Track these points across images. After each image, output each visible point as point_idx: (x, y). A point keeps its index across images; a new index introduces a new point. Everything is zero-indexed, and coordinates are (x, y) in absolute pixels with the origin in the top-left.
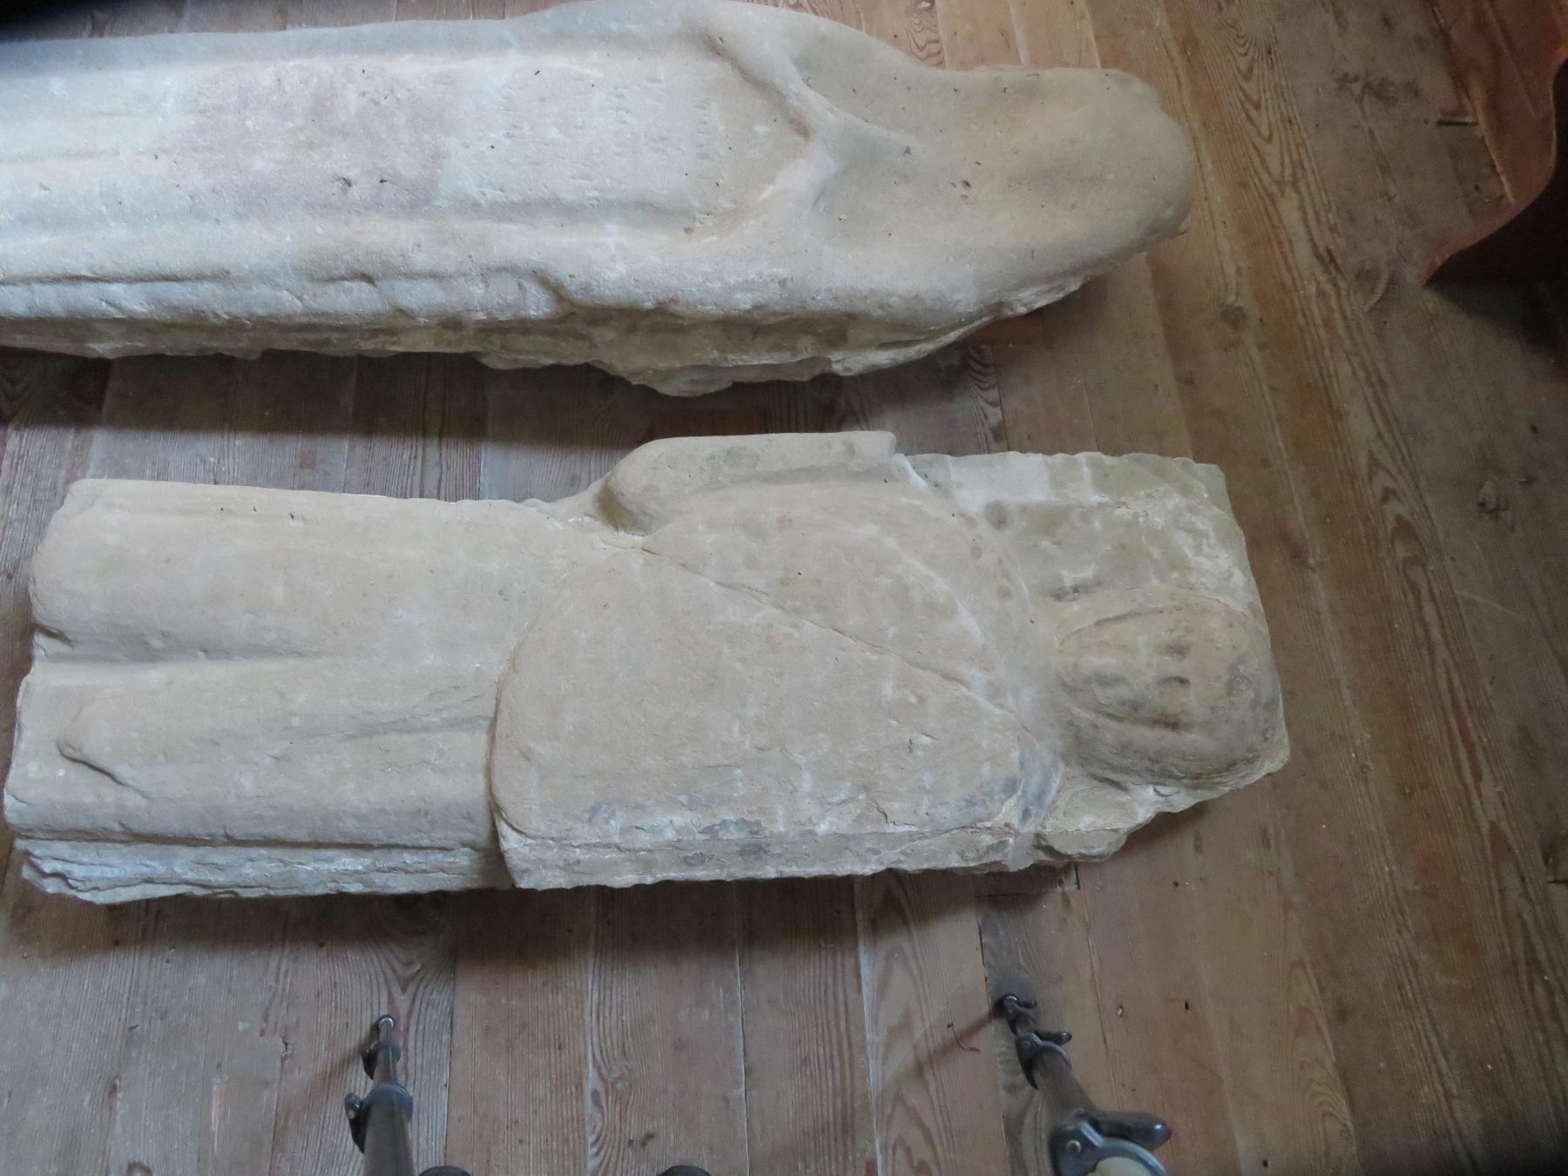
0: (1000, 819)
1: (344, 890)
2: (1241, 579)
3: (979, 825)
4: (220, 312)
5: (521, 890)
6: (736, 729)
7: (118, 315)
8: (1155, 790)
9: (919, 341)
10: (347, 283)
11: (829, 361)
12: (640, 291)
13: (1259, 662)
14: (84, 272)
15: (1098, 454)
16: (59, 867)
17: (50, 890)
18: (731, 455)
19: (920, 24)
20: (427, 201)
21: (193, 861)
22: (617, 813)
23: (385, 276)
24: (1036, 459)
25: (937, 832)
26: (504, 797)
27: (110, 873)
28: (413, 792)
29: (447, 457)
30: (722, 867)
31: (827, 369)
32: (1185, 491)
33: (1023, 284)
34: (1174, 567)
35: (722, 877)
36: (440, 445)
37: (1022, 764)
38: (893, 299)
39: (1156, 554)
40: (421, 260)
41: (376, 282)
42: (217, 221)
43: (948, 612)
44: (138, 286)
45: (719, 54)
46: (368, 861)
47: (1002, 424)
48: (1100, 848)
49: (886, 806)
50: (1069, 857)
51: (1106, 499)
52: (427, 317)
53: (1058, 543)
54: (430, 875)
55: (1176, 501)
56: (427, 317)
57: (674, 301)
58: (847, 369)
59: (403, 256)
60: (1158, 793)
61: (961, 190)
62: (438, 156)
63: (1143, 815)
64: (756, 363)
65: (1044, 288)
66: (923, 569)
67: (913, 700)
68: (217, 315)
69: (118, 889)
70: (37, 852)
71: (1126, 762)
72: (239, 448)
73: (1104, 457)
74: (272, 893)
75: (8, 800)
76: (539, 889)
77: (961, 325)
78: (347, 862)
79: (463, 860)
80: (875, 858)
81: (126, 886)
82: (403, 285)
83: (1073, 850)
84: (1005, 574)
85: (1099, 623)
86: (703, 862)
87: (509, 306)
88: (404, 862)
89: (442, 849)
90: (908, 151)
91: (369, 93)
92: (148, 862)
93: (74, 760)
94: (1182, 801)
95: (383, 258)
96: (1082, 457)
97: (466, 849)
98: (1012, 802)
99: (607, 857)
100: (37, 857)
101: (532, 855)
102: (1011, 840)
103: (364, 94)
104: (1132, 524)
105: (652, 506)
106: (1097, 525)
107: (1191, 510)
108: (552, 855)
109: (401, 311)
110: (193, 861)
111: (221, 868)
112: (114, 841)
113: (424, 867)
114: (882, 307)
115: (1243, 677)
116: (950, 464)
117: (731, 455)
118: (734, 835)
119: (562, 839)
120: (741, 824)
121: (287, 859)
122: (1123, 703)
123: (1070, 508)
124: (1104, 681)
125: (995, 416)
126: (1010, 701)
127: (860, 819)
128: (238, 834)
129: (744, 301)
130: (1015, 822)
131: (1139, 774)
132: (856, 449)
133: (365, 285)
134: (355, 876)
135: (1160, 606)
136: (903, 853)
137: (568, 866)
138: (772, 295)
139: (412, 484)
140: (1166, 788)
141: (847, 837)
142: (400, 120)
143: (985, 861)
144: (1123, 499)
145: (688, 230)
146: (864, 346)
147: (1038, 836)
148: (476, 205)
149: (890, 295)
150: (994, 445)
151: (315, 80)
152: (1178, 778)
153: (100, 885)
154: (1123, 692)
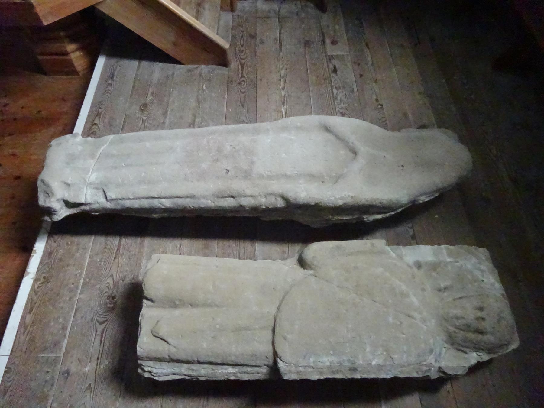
0: (428, 361)
1: (230, 379)
2: (498, 285)
3: (422, 363)
4: (191, 206)
5: (284, 379)
6: (346, 331)
7: (163, 207)
8: (476, 354)
9: (390, 212)
10: (227, 198)
11: (363, 218)
12: (311, 200)
13: (507, 313)
14: (156, 196)
15: (447, 246)
16: (149, 369)
17: (146, 376)
18: (338, 248)
21: (187, 369)
22: (312, 357)
23: (238, 196)
24: (429, 247)
25: (409, 365)
26: (279, 351)
27: (164, 371)
28: (251, 349)
29: (246, 246)
30: (344, 374)
31: (363, 220)
32: (477, 258)
33: (421, 195)
34: (475, 281)
35: (344, 377)
36: (244, 242)
37: (434, 344)
38: (384, 201)
39: (469, 277)
40: (248, 192)
41: (236, 198)
42: (192, 181)
43: (407, 296)
44: (170, 199)
46: (237, 370)
47: (414, 234)
48: (460, 372)
49: (393, 356)
50: (450, 375)
51: (451, 260)
52: (248, 207)
54: (255, 374)
55: (474, 260)
56: (248, 207)
57: (320, 203)
58: (368, 220)
59: (243, 191)
60: (478, 355)
61: (402, 168)
62: (252, 163)
63: (473, 362)
64: (342, 219)
65: (428, 196)
66: (398, 282)
67: (399, 323)
68: (190, 207)
69: (165, 376)
70: (144, 365)
71: (466, 344)
72: (186, 243)
73: (450, 246)
74: (208, 379)
75: (138, 348)
76: (289, 380)
77: (403, 207)
78: (231, 370)
79: (264, 370)
80: (390, 373)
81: (168, 375)
82: (243, 198)
83: (451, 373)
84: (423, 283)
85: (454, 300)
86: (338, 373)
87: (272, 204)
88: (247, 370)
89: (259, 366)
90: (385, 157)
92: (174, 368)
93: (156, 337)
94: (485, 357)
95: (238, 191)
96: (443, 246)
97: (265, 367)
98: (432, 356)
99: (309, 370)
100: (143, 366)
101: (287, 369)
102: (432, 369)
103: (231, 146)
104: (461, 267)
105: (315, 262)
106: (450, 268)
107: (480, 263)
108: (293, 369)
109: (241, 206)
110: (187, 369)
111: (194, 370)
112: (165, 362)
113: (253, 372)
114: (380, 203)
115: (503, 318)
116: (402, 249)
117: (338, 248)
118: (347, 364)
119: (295, 364)
120: (349, 361)
121: (214, 368)
122: (464, 325)
123: (440, 263)
124: (457, 318)
125: (411, 232)
126: (429, 324)
127: (385, 360)
128: (201, 360)
129: (340, 203)
130: (433, 363)
131: (471, 348)
132: (375, 245)
133: (232, 199)
134: (233, 374)
136: (399, 371)
137: (298, 373)
138: (349, 201)
139: (236, 254)
140: (480, 353)
141: (383, 366)
142: (241, 153)
143: (425, 375)
144: (457, 260)
145: (323, 182)
146: (374, 214)
147: (440, 368)
148: (263, 176)
149: (383, 200)
150: (412, 242)
151: (218, 142)
152: (483, 350)
153: (161, 375)
154: (464, 322)
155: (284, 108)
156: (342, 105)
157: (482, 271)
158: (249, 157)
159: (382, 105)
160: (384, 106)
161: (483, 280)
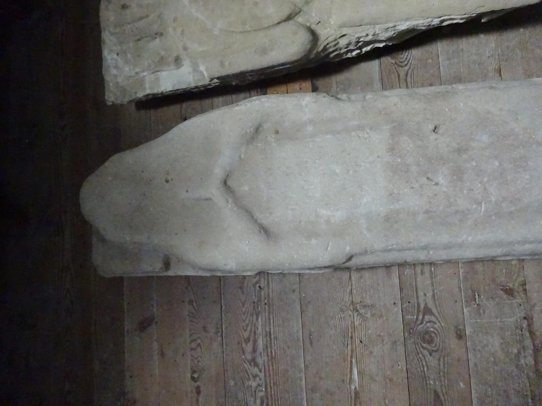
18: (264, 52)
19: (199, 361)
20: (394, 127)
45: (263, 227)
53: (159, 54)
55: (120, 80)
61: (169, 178)
62: (392, 149)
85: (147, 16)
91: (434, 185)
103: (437, 184)
107: (115, 76)
117: (264, 52)
135: (129, 26)
142: (414, 168)
151: (465, 192)
155: (355, 385)
156: (254, 384)
157: (116, 67)
158: (399, 160)
159: (193, 378)
160: (189, 375)
161: (118, 54)
